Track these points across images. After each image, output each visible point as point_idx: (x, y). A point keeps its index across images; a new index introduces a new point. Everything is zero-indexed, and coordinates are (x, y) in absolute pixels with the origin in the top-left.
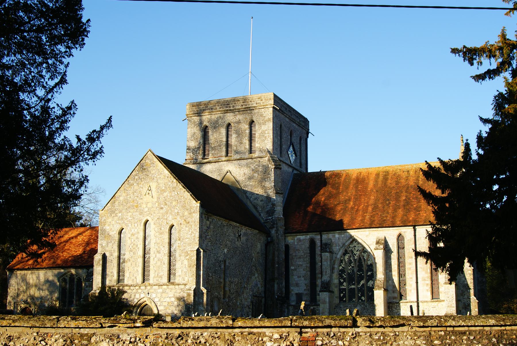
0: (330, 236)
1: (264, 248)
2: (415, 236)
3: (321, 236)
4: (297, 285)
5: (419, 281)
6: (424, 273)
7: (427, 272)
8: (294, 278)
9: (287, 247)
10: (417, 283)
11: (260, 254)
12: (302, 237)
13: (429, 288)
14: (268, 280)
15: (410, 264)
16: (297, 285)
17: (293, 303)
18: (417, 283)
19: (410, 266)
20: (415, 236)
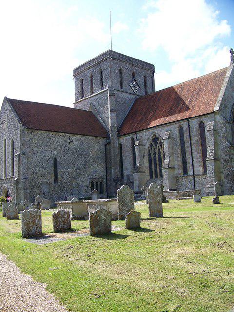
0: (141, 134)
1: (103, 147)
2: (189, 126)
3: (136, 135)
4: (127, 169)
5: (194, 160)
6: (197, 153)
7: (199, 153)
8: (125, 165)
9: (121, 145)
10: (192, 161)
11: (99, 152)
12: (127, 137)
13: (201, 164)
14: (107, 168)
15: (188, 147)
16: (127, 169)
17: (125, 182)
18: (192, 161)
19: (188, 149)
20: (189, 126)
